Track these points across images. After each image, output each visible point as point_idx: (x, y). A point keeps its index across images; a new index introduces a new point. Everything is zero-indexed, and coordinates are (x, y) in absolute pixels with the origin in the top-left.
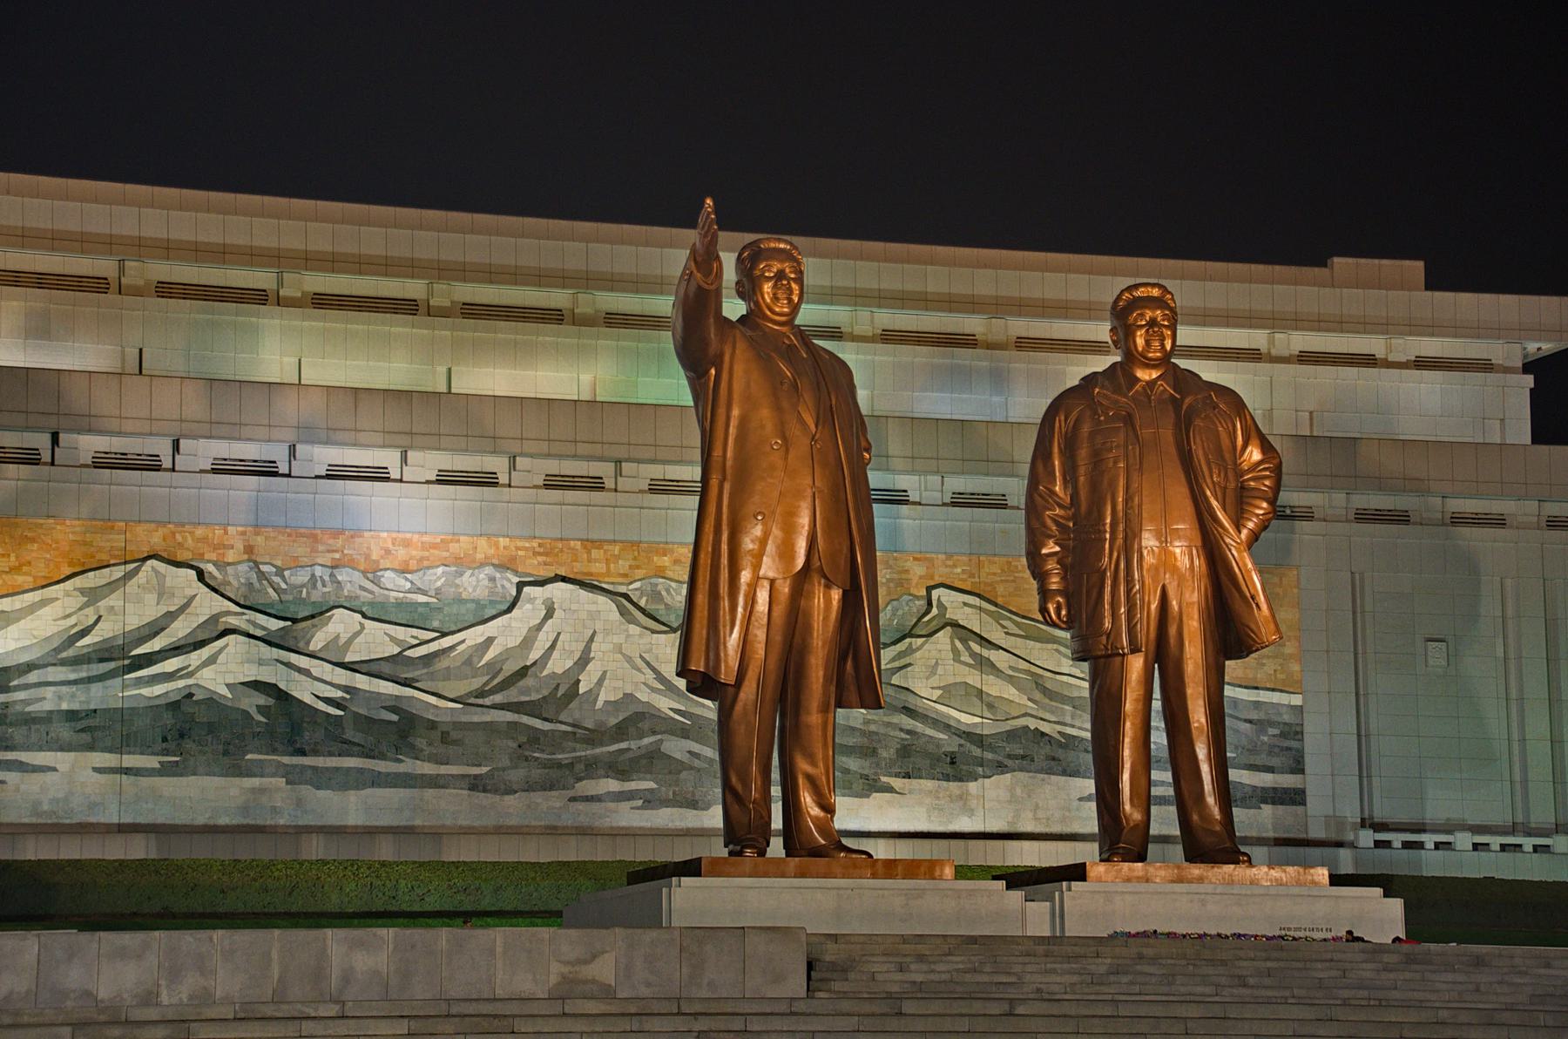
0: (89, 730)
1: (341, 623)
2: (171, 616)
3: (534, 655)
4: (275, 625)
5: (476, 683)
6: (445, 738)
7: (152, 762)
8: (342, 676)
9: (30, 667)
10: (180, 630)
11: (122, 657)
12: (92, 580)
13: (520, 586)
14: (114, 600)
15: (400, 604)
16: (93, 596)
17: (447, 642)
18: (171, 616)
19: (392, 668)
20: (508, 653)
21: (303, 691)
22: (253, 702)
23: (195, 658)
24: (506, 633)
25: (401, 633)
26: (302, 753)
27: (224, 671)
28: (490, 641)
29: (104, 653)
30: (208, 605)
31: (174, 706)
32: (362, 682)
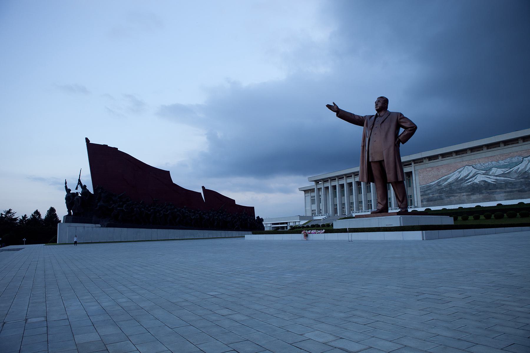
0: (461, 190)
1: (494, 170)
2: (470, 173)
3: (527, 169)
4: (484, 172)
5: (517, 175)
6: (513, 185)
7: (470, 194)
8: (495, 178)
9: (453, 183)
10: (471, 175)
11: (463, 180)
12: (459, 170)
13: (523, 159)
14: (462, 172)
15: (503, 165)
16: (460, 172)
17: (511, 170)
18: (470, 173)
19: (503, 175)
20: (522, 170)
21: (489, 181)
22: (482, 183)
23: (474, 178)
24: (521, 167)
25: (503, 169)
26: (490, 190)
27: (479, 179)
28: (519, 168)
29: (462, 179)
30: (474, 171)
31: (471, 185)
32: (498, 178)
